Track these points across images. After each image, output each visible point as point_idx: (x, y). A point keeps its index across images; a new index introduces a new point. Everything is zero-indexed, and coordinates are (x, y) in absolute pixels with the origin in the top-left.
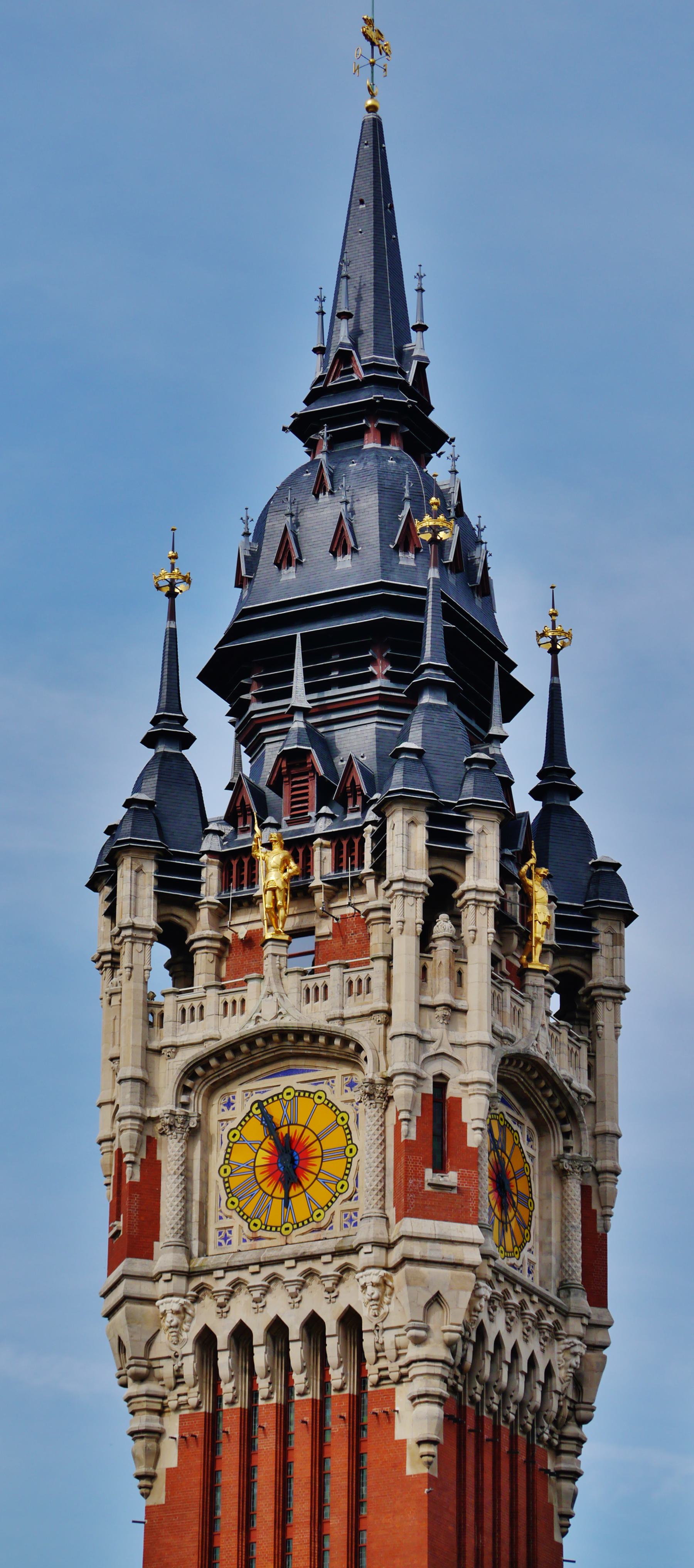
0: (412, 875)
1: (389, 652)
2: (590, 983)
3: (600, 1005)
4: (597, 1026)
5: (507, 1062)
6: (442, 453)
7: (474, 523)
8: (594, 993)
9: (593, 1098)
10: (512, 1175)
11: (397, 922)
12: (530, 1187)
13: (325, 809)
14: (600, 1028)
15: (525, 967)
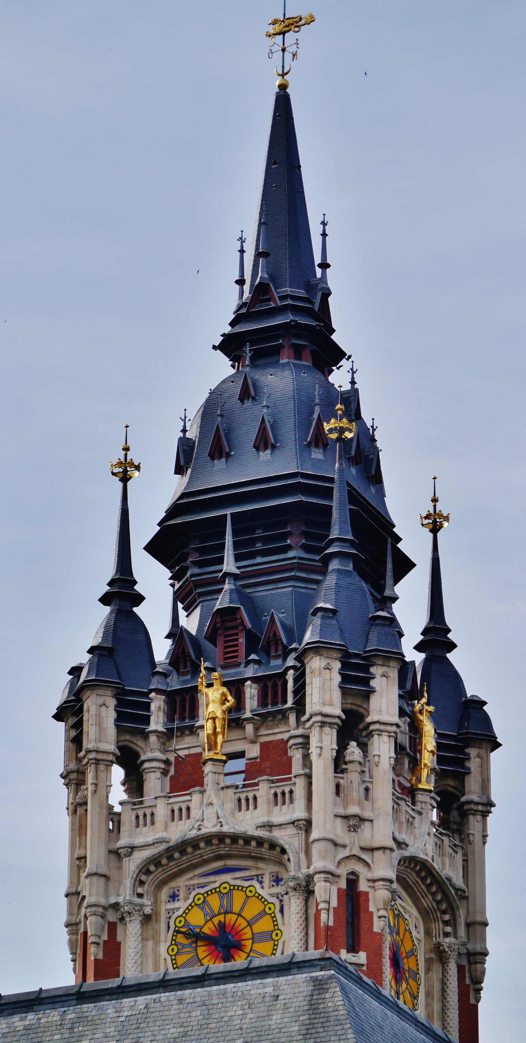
0: (328, 710)
1: (303, 529)
2: (463, 799)
3: (471, 817)
4: (469, 835)
5: (402, 862)
6: (340, 367)
7: (369, 425)
8: (466, 807)
9: (466, 894)
10: (404, 955)
11: (316, 748)
12: (418, 965)
13: (253, 657)
14: (471, 836)
15: (415, 787)
